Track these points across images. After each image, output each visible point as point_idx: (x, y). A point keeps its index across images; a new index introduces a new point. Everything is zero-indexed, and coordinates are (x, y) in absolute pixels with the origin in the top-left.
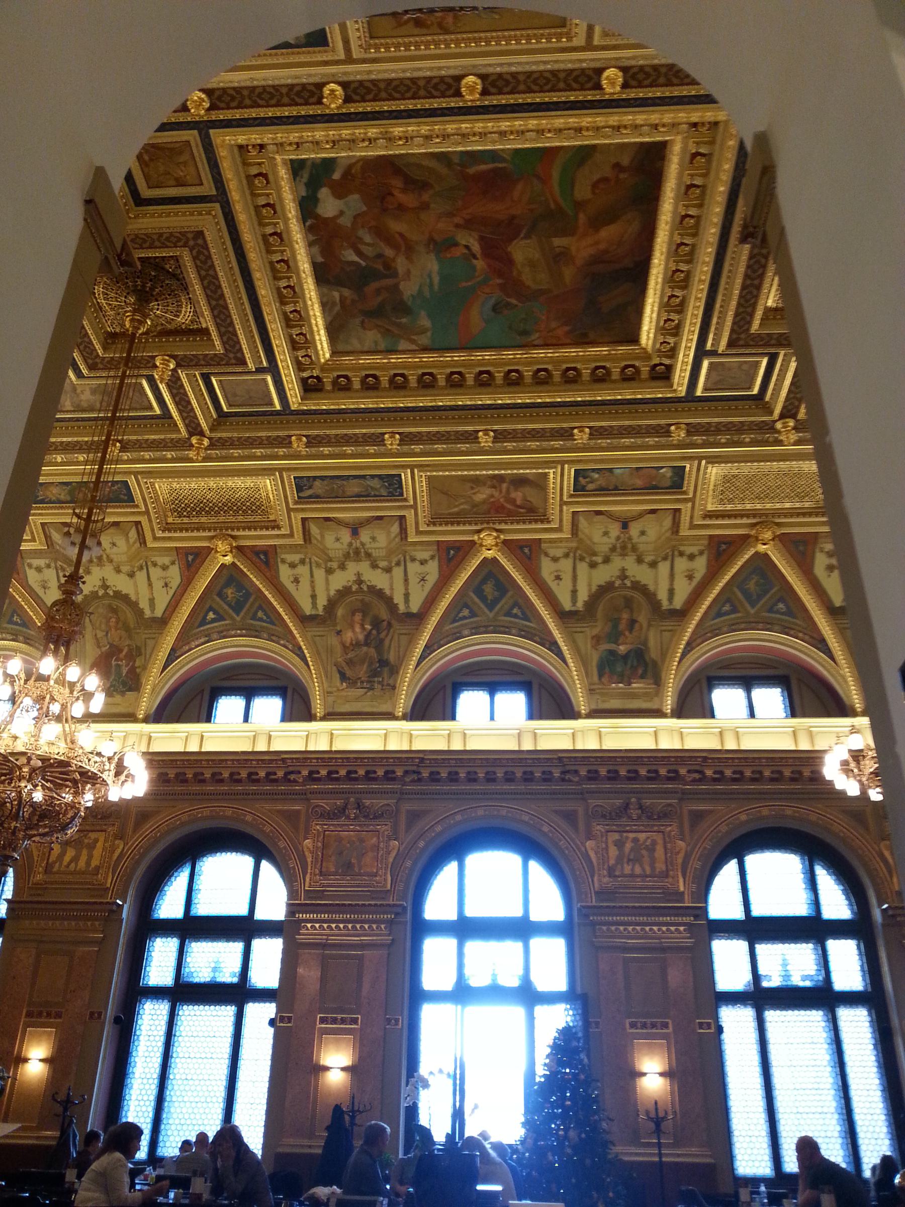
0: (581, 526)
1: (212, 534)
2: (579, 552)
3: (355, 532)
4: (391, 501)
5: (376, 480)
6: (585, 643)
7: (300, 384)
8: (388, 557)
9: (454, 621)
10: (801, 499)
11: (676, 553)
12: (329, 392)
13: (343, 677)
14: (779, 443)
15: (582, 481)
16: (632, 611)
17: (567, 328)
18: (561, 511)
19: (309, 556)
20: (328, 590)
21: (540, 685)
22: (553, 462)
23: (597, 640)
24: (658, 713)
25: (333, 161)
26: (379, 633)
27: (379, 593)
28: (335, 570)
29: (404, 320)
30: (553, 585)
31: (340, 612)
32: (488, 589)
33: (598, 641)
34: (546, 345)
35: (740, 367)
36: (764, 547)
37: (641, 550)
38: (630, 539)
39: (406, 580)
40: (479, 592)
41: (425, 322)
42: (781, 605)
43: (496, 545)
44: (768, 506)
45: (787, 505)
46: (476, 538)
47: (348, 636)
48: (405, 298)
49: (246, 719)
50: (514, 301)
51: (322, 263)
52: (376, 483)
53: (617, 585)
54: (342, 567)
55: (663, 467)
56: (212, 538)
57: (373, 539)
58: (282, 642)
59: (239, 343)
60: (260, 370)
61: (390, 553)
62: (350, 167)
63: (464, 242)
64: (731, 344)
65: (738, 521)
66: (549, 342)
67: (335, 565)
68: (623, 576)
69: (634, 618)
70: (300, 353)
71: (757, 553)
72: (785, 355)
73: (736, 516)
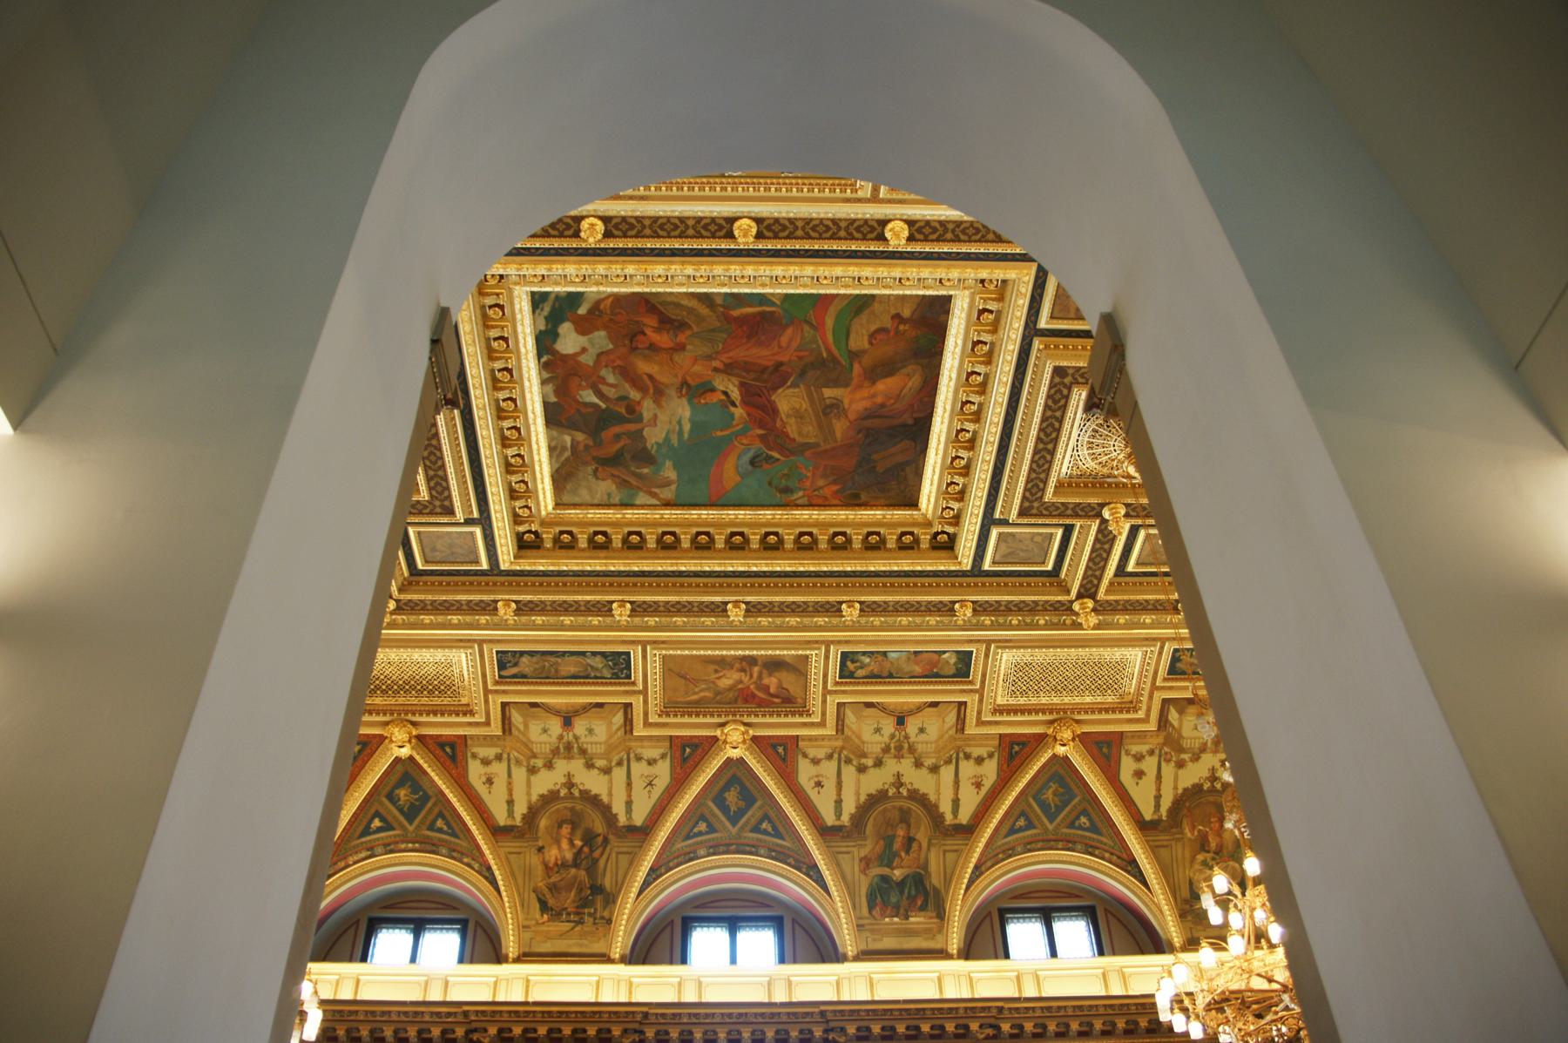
0: (847, 721)
1: (387, 718)
2: (845, 752)
3: (567, 722)
4: (615, 684)
5: (598, 659)
6: (851, 865)
7: (515, 540)
8: (607, 755)
9: (688, 837)
10: (1104, 693)
11: (961, 755)
12: (548, 549)
13: (544, 907)
14: (1079, 626)
16: (909, 826)
17: (835, 488)
18: (824, 701)
19: (508, 749)
20: (529, 794)
21: (794, 921)
22: (817, 642)
23: (866, 862)
24: (941, 954)
25: (580, 294)
26: (592, 851)
27: (593, 800)
28: (539, 770)
29: (645, 471)
30: (812, 794)
31: (543, 823)
32: (732, 797)
33: (867, 865)
34: (811, 505)
35: (1032, 539)
36: (1063, 748)
37: (919, 750)
38: (907, 737)
39: (629, 784)
40: (720, 802)
41: (669, 472)
42: (1083, 820)
43: (744, 742)
44: (1066, 700)
45: (1088, 699)
46: (718, 733)
47: (552, 854)
48: (649, 446)
49: (413, 960)
50: (776, 455)
51: (554, 403)
52: (598, 662)
53: (890, 794)
54: (549, 765)
55: (945, 652)
56: (387, 724)
57: (590, 731)
58: (466, 860)
59: (448, 488)
60: (468, 522)
61: (611, 748)
62: (598, 303)
63: (722, 388)
64: (1022, 513)
65: (1033, 718)
66: (814, 502)
67: (539, 763)
68: (899, 783)
69: (911, 835)
70: (518, 504)
71: (1055, 756)
72: (1081, 526)
73: (1030, 712)
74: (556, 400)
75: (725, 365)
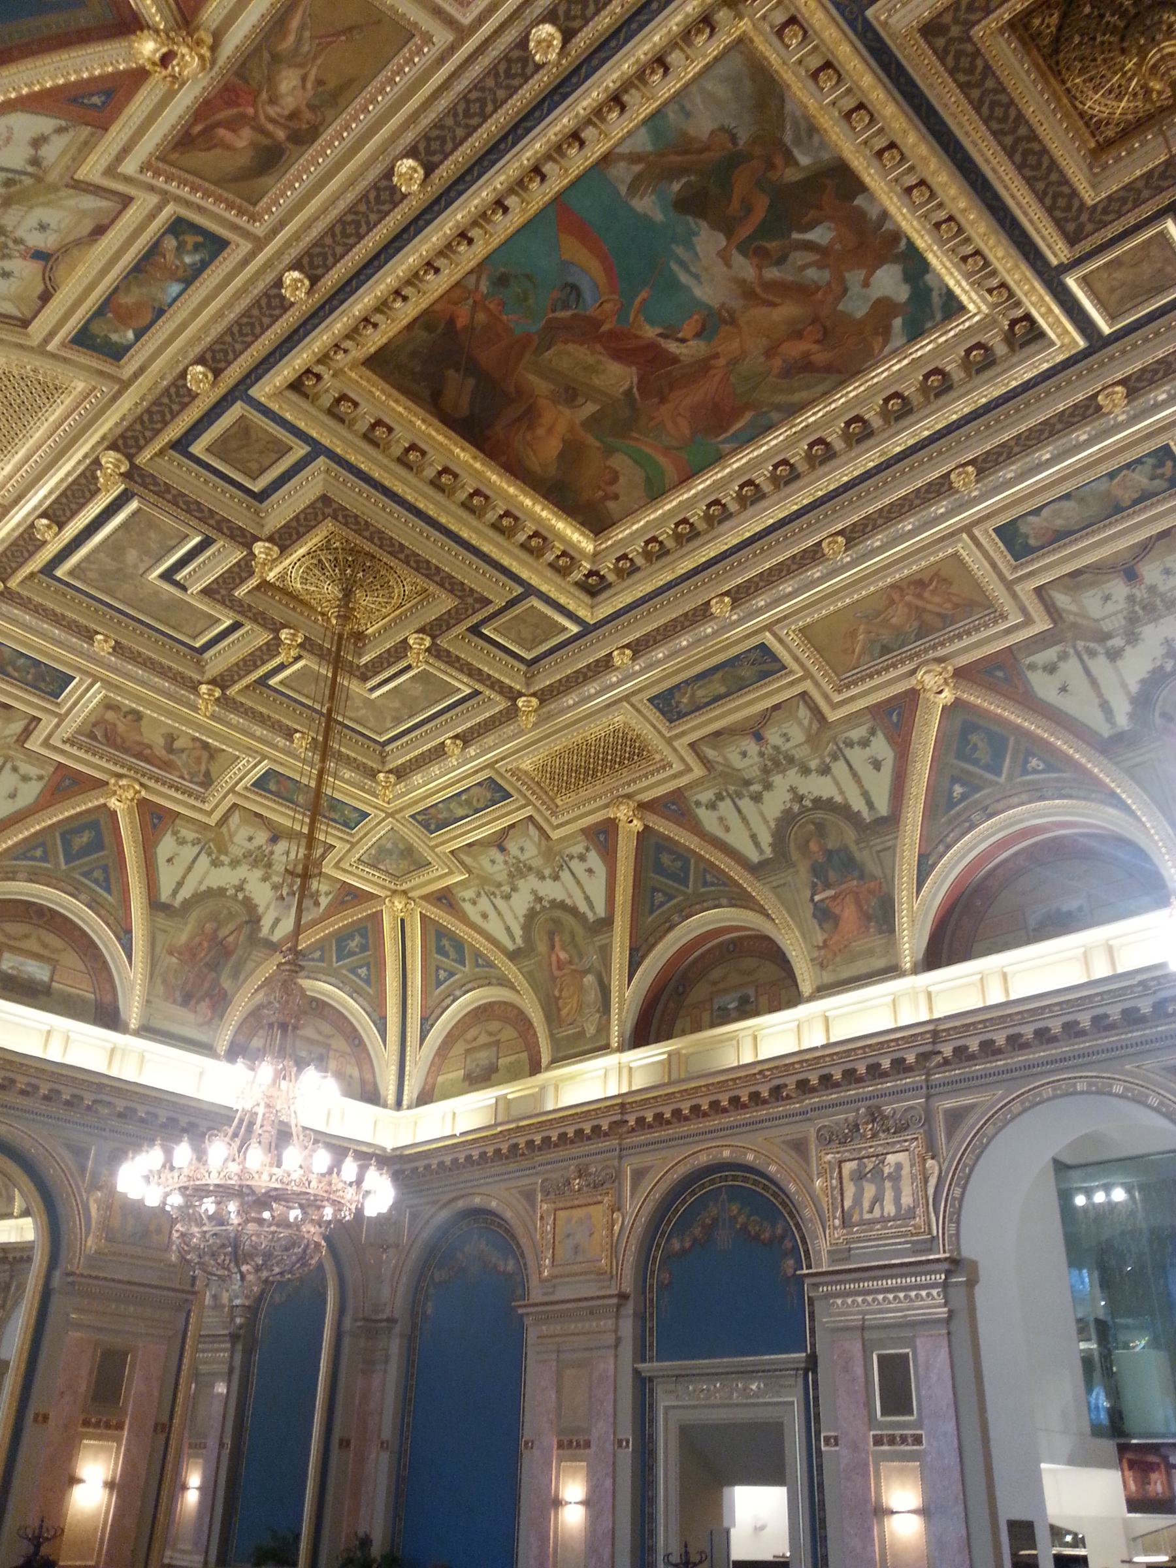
15: (191, 240)
29: (676, 187)
41: (646, 204)
48: (704, 224)
51: (854, 198)
62: (886, 342)
63: (690, 343)
74: (856, 202)
75: (711, 368)
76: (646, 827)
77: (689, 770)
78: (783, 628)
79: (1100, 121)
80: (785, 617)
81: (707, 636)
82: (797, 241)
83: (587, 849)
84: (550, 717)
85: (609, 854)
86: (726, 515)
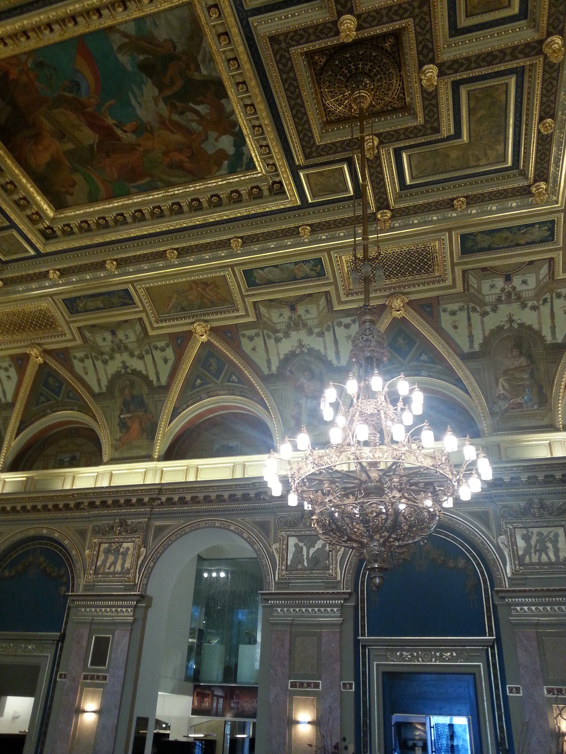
29: (141, 57)
41: (124, 59)
48: (150, 81)
50: (66, 94)
51: (221, 99)
62: (219, 169)
63: (129, 134)
76: (45, 362)
77: (74, 339)
78: (138, 285)
79: (330, 111)
80: (141, 280)
81: (100, 277)
82: (191, 107)
83: (10, 366)
84: (8, 293)
85: (21, 372)
86: (125, 222)
